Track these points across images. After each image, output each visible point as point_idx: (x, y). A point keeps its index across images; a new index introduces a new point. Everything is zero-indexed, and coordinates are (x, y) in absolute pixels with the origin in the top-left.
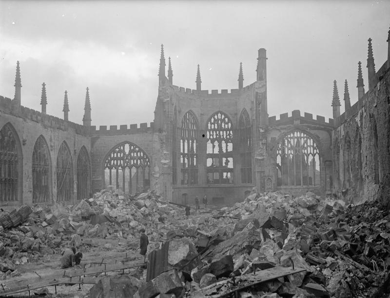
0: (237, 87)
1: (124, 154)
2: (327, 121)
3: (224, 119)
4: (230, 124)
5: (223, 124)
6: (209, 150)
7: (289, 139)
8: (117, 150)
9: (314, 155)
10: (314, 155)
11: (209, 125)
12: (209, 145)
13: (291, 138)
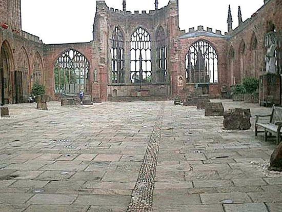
1: (69, 58)
2: (223, 33)
4: (148, 37)
5: (143, 37)
6: (133, 58)
7: (195, 47)
8: (64, 55)
11: (133, 37)
12: (133, 52)
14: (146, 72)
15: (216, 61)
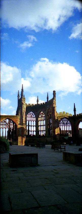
0: (36, 103)
1: (6, 123)
3: (33, 114)
4: (35, 116)
5: (32, 115)
9: (70, 126)
10: (70, 126)
13: (63, 120)
14: (33, 131)
15: (71, 127)
